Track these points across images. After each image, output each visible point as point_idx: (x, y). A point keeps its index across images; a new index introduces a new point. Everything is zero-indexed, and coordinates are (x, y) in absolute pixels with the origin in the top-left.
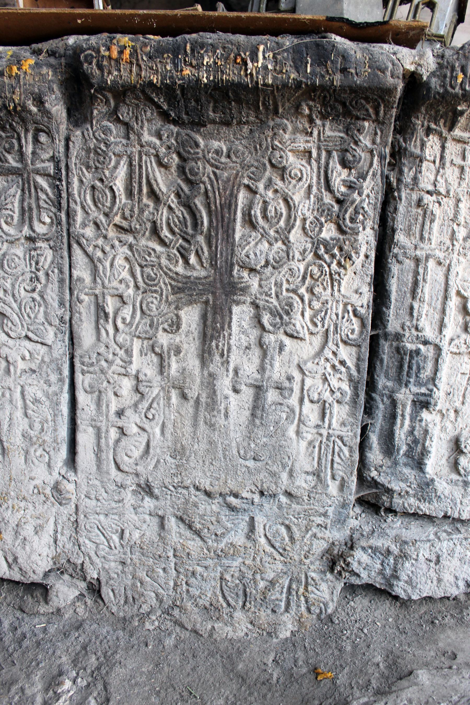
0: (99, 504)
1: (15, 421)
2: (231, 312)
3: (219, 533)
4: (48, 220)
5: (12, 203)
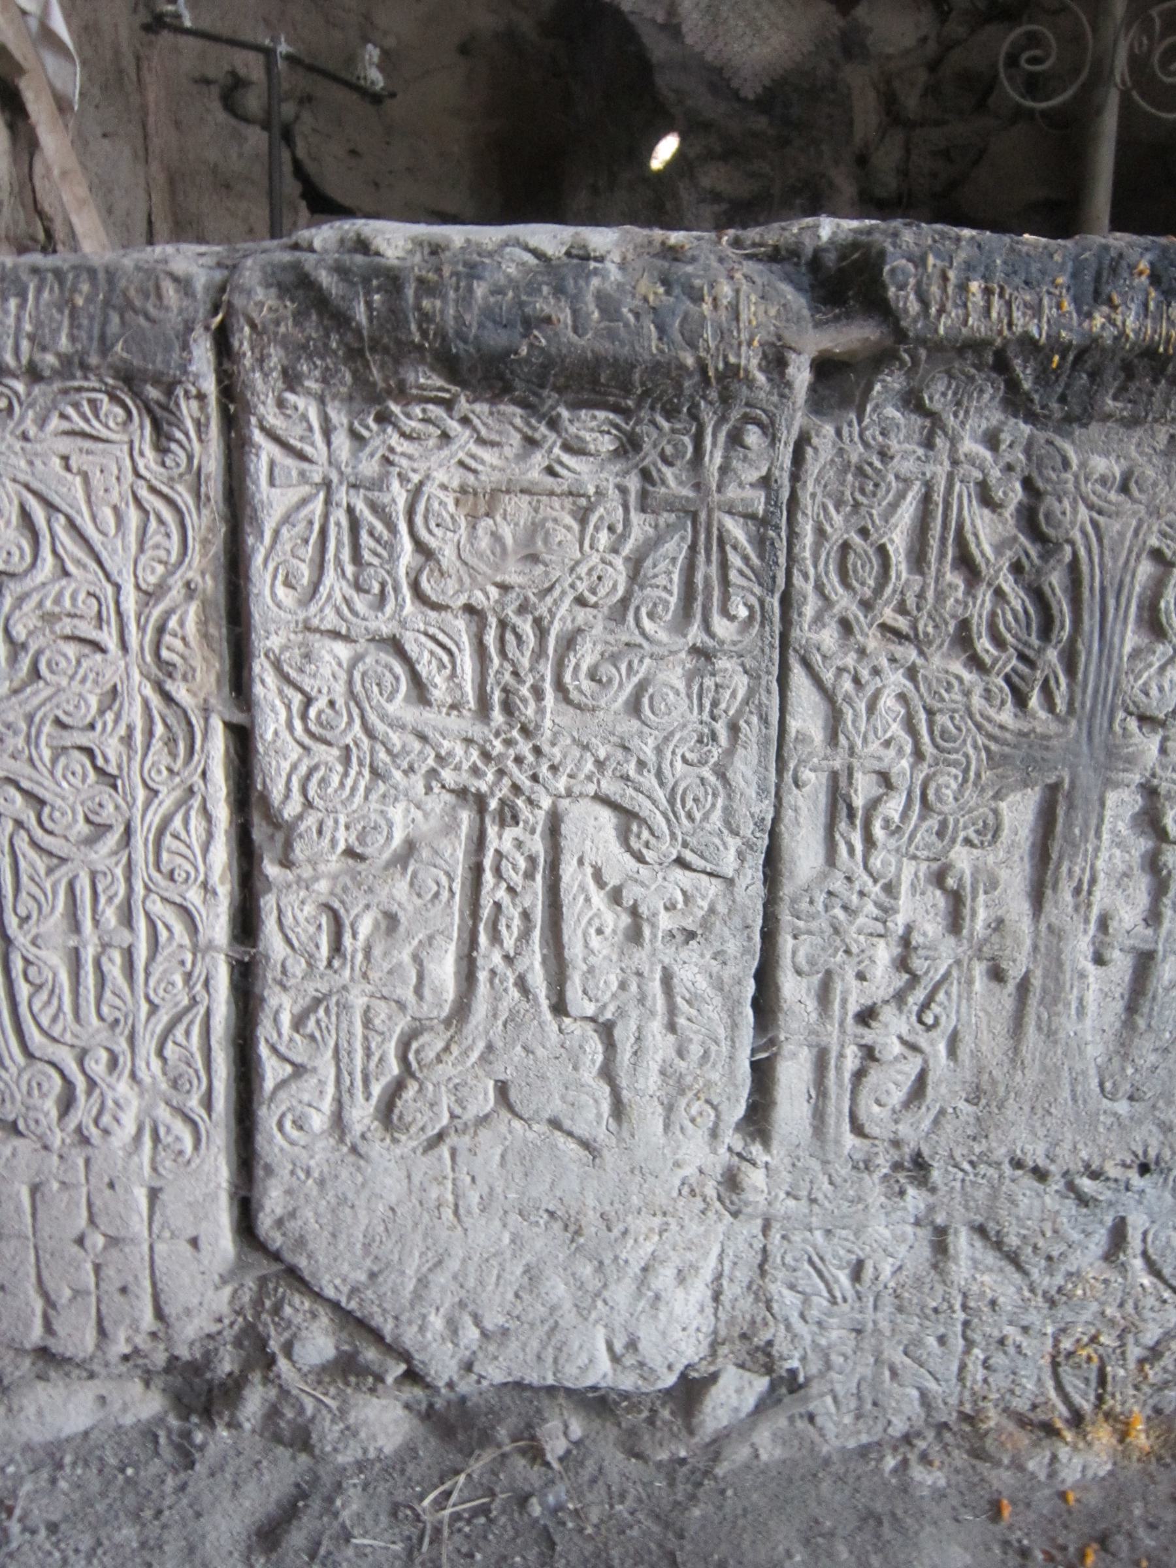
0: (816, 1208)
1: (649, 1042)
2: (1102, 804)
3: (1055, 1254)
4: (743, 613)
5: (669, 573)
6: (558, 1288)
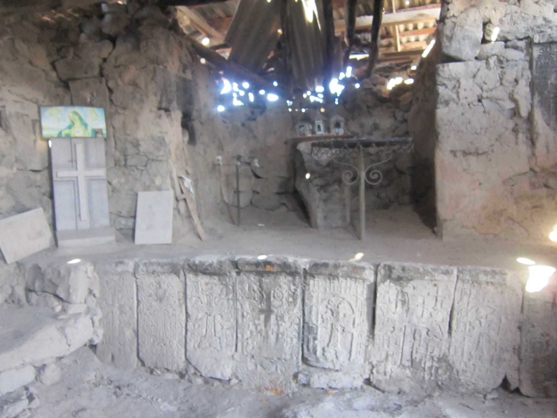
6: (215, 366)
